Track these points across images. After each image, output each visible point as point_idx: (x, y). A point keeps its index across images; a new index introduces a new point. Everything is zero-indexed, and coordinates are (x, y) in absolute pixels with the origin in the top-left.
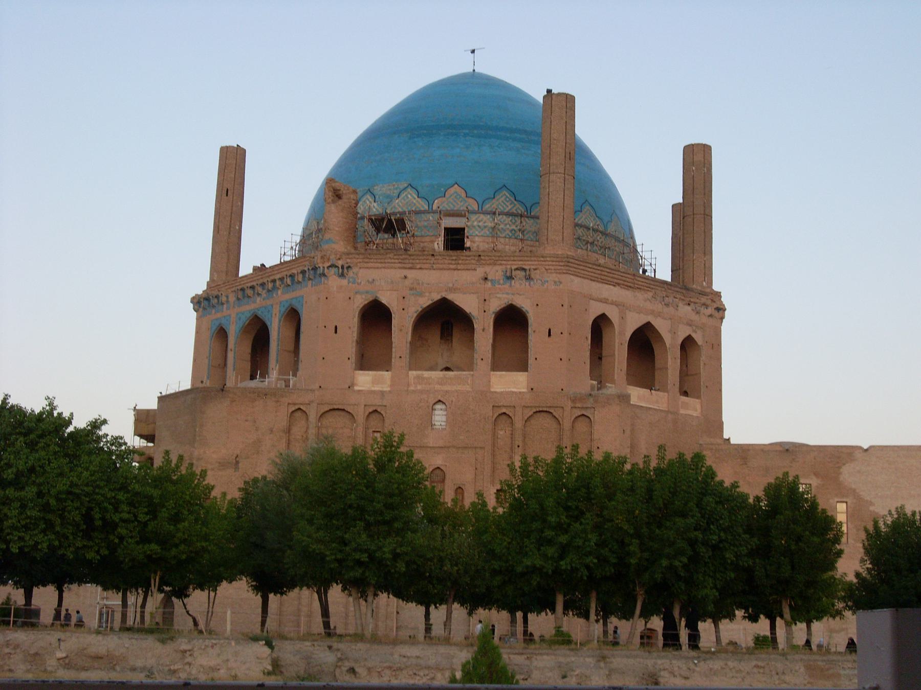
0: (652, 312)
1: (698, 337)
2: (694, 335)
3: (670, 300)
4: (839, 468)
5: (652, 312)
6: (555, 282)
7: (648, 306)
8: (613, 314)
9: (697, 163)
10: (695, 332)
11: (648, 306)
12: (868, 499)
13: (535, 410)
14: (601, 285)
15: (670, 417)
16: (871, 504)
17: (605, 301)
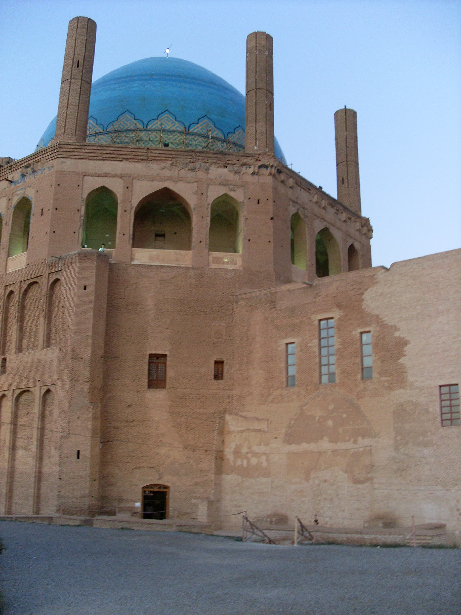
0: (170, 179)
1: (238, 195)
2: (232, 194)
3: (198, 165)
4: (362, 294)
5: (170, 179)
6: (49, 168)
7: (167, 173)
8: (116, 187)
9: (260, 51)
10: (232, 190)
11: (167, 173)
12: (393, 324)
13: (28, 282)
14: (101, 162)
15: (192, 272)
16: (396, 329)
17: (105, 175)
